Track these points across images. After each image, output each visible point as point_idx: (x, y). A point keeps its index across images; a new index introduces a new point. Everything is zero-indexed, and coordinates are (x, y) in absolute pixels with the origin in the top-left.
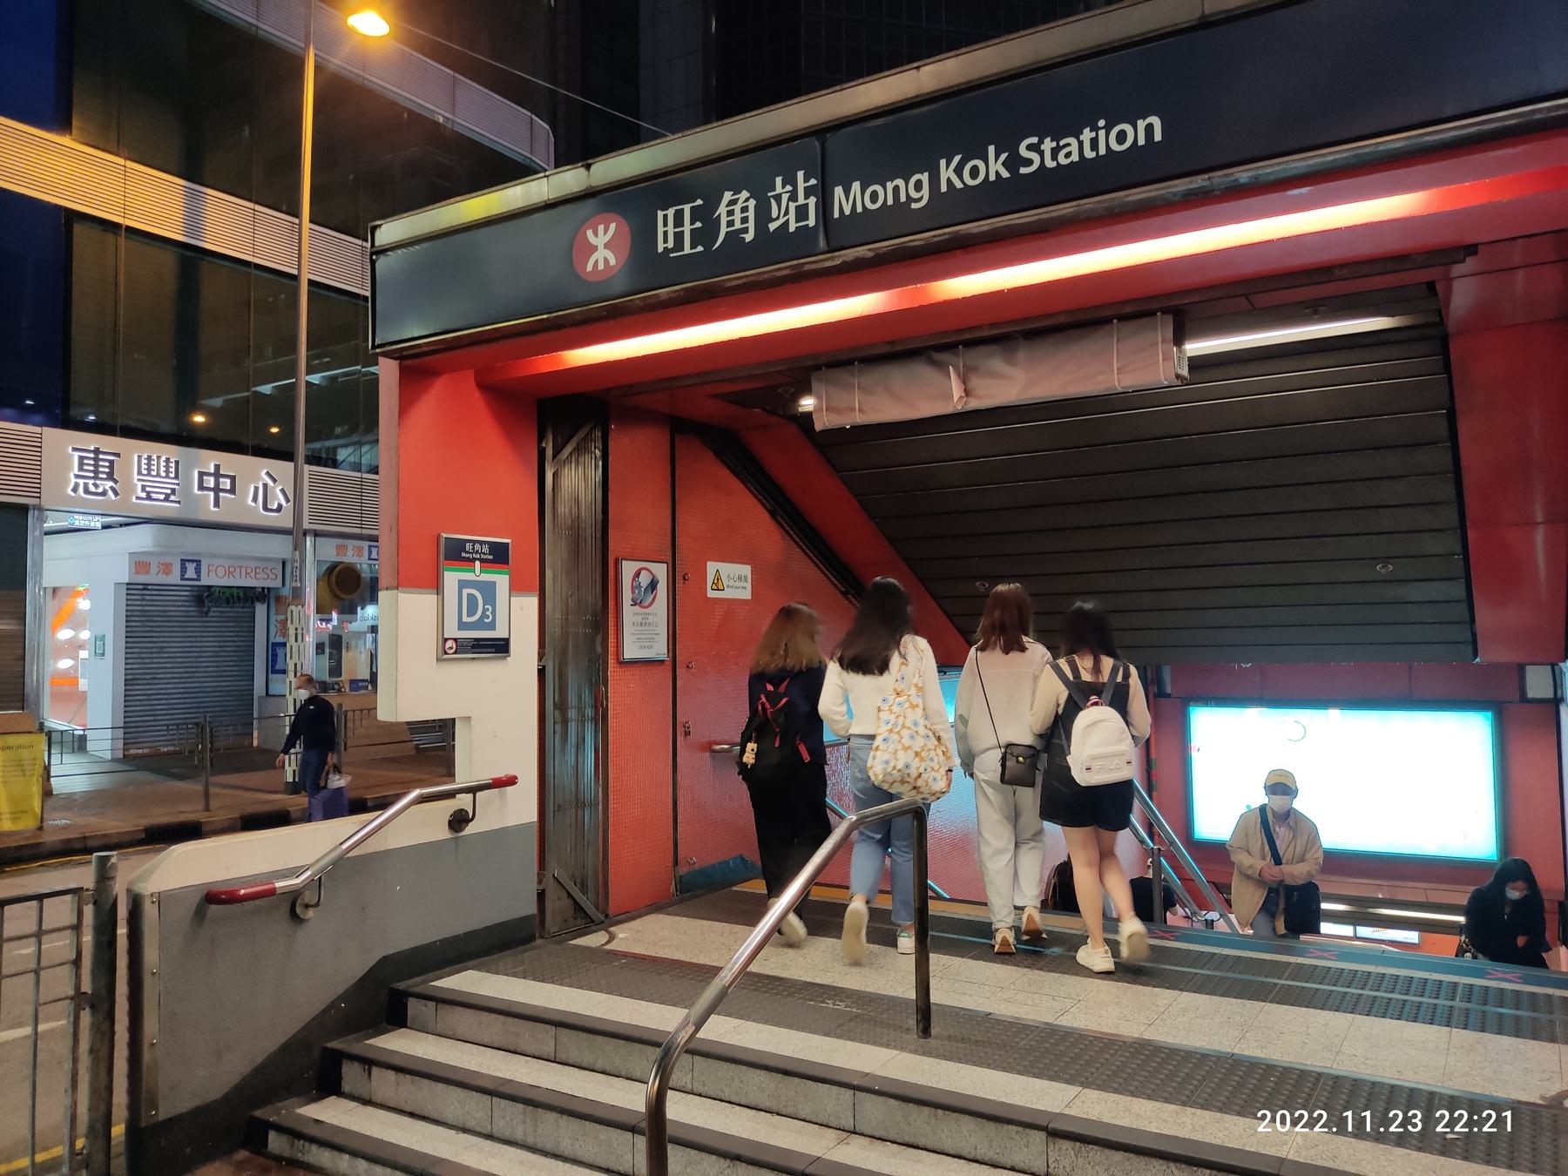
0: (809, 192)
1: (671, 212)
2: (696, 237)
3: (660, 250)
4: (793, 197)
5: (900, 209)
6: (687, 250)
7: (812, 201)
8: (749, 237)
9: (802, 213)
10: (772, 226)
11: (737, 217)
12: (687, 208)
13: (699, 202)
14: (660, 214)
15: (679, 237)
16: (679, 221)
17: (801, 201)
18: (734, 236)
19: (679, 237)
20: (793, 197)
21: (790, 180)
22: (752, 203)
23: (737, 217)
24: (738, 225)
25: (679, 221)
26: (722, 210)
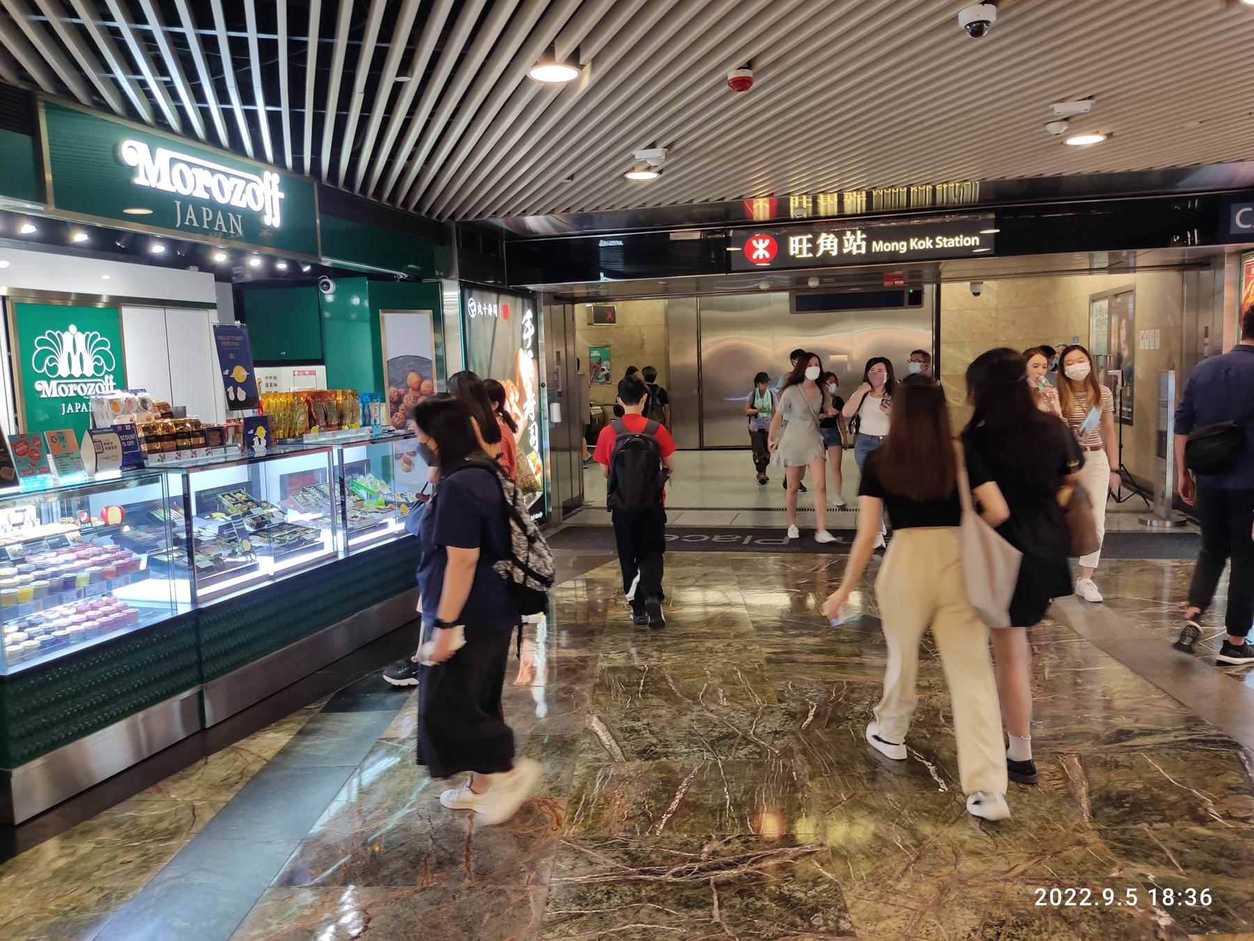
0: (862, 239)
1: (797, 239)
2: (809, 250)
3: (792, 253)
4: (855, 240)
5: (895, 253)
6: (805, 255)
7: (864, 244)
8: (834, 253)
9: (859, 247)
10: (845, 251)
11: (829, 245)
12: (804, 238)
13: (810, 236)
14: (792, 239)
15: (801, 250)
16: (801, 242)
17: (859, 242)
18: (826, 253)
19: (801, 250)
20: (855, 240)
21: (854, 233)
22: (836, 240)
23: (829, 245)
24: (829, 248)
25: (801, 242)
26: (821, 241)
